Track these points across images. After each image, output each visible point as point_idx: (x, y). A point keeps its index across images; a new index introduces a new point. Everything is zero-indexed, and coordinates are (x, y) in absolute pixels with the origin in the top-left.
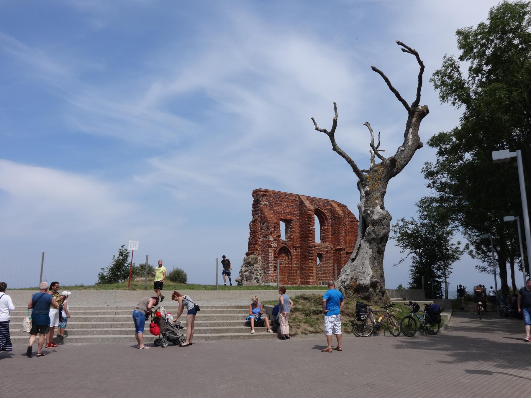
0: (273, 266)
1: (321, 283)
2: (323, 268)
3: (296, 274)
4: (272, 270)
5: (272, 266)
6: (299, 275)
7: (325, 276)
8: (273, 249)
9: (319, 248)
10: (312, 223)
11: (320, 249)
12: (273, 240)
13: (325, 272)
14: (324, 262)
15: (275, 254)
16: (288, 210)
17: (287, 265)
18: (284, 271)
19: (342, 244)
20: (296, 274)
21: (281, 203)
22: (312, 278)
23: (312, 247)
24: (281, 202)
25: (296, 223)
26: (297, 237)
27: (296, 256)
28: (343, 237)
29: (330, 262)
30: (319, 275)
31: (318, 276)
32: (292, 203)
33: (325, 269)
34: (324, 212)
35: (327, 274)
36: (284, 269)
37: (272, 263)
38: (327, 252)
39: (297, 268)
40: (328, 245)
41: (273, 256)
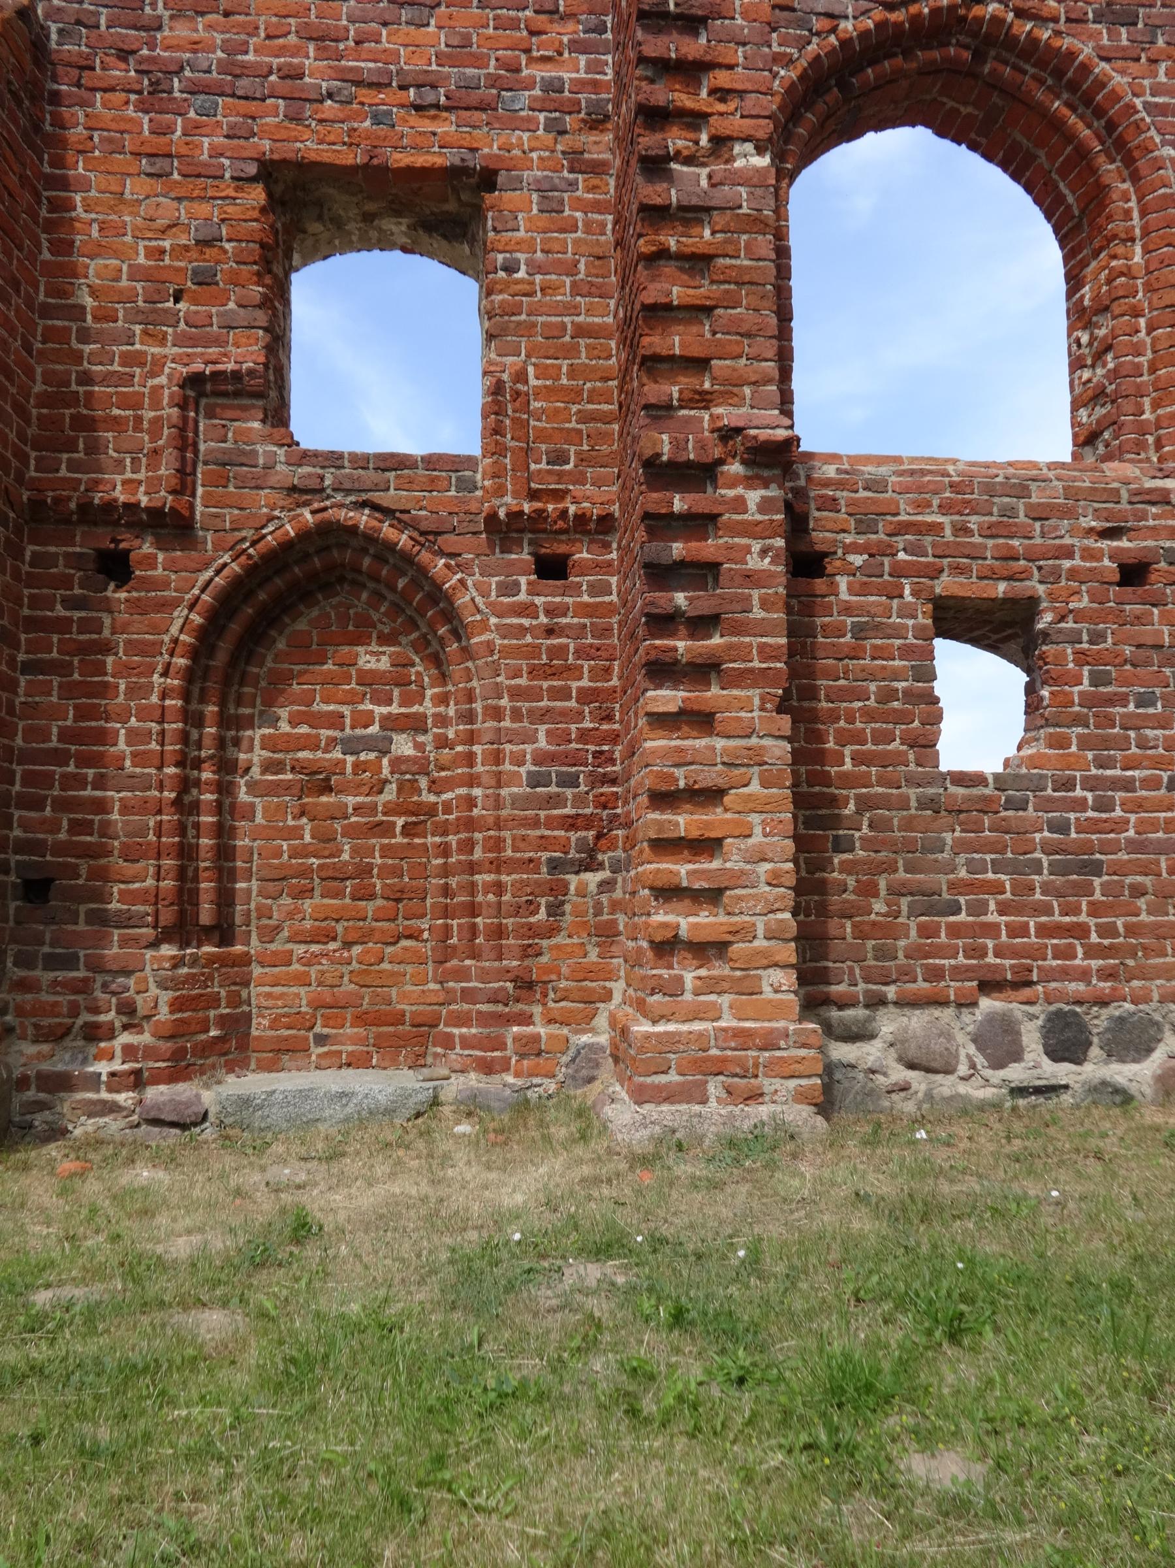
1: (1031, 1038)
2: (1046, 805)
3: (555, 910)
6: (607, 934)
7: (1107, 931)
9: (962, 529)
11: (990, 532)
13: (1096, 869)
14: (1079, 720)
17: (436, 786)
18: (385, 871)
20: (555, 910)
22: (710, 986)
25: (551, 208)
26: (575, 395)
27: (561, 651)
30: (979, 909)
31: (955, 931)
33: (1093, 826)
34: (1072, 55)
35: (1138, 891)
36: (386, 851)
39: (571, 823)
40: (1149, 484)
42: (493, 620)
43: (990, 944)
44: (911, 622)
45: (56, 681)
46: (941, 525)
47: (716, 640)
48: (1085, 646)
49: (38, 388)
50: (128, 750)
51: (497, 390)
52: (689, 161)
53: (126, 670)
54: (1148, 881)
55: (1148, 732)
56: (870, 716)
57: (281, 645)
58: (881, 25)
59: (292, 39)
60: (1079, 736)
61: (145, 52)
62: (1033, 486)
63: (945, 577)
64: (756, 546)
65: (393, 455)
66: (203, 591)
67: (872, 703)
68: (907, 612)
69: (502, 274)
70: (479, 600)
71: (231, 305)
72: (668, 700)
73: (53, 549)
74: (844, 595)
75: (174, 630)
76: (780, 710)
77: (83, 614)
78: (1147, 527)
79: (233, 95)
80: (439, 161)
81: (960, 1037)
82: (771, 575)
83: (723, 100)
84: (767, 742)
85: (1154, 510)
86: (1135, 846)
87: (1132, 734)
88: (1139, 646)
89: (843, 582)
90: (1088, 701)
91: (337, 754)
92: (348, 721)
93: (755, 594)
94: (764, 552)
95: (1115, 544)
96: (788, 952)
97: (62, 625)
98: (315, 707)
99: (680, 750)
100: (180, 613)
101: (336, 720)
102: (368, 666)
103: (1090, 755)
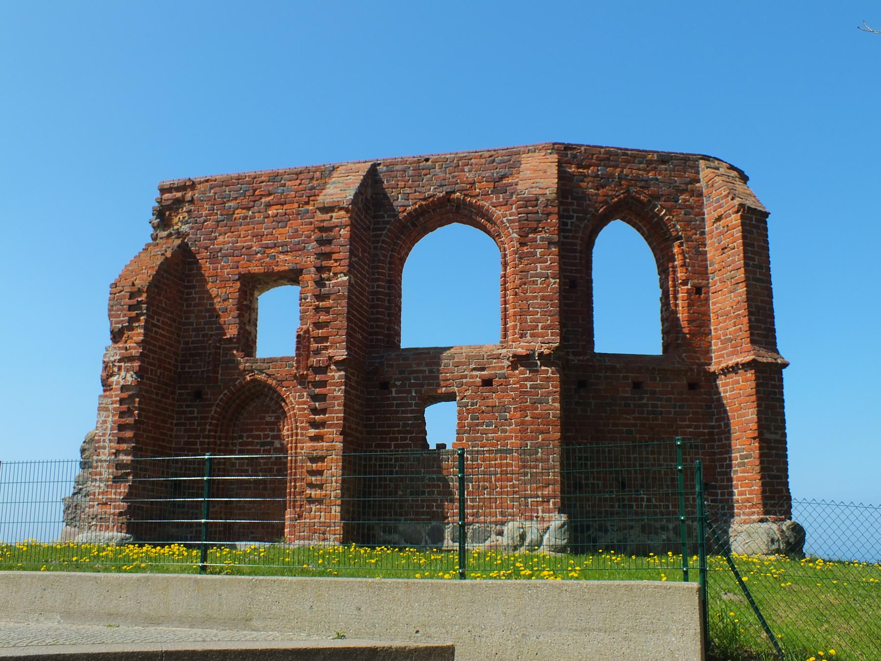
0: (109, 461)
4: (101, 481)
5: (105, 464)
8: (116, 396)
10: (336, 261)
12: (120, 361)
15: (122, 414)
16: (283, 234)
19: (532, 335)
21: (250, 212)
23: (323, 370)
24: (248, 209)
28: (543, 298)
29: (505, 431)
30: (431, 493)
32: (307, 203)
34: (483, 207)
35: (485, 488)
37: (107, 451)
38: (487, 382)
41: (114, 422)
42: (297, 406)
43: (434, 504)
44: (414, 402)
45: (183, 428)
46: (425, 371)
47: (327, 415)
48: (469, 407)
49: (182, 346)
50: (200, 447)
51: (298, 336)
52: (329, 279)
53: (199, 424)
54: (487, 484)
55: (490, 435)
56: (399, 432)
57: (245, 415)
58: (420, 206)
59: (249, 237)
60: (466, 437)
61: (211, 247)
62: (456, 355)
63: (425, 387)
64: (337, 389)
65: (271, 358)
66: (220, 401)
67: (400, 428)
68: (413, 398)
69: (303, 300)
70: (293, 400)
71: (230, 318)
72: (312, 432)
73: (183, 391)
74: (394, 394)
75: (212, 413)
76: (341, 434)
77: (190, 409)
78: (492, 367)
79: (233, 256)
80: (287, 268)
81: (424, 534)
82: (341, 397)
83: (336, 262)
84: (337, 443)
85: (495, 361)
86: (484, 473)
87: (484, 436)
88: (487, 407)
89: (394, 390)
90: (469, 425)
91: (258, 447)
92: (262, 437)
93: (336, 402)
94: (339, 390)
95: (482, 373)
96: (339, 502)
97: (184, 412)
98: (253, 433)
99: (314, 446)
100: (214, 408)
101: (259, 437)
102: (269, 420)
103: (470, 443)
